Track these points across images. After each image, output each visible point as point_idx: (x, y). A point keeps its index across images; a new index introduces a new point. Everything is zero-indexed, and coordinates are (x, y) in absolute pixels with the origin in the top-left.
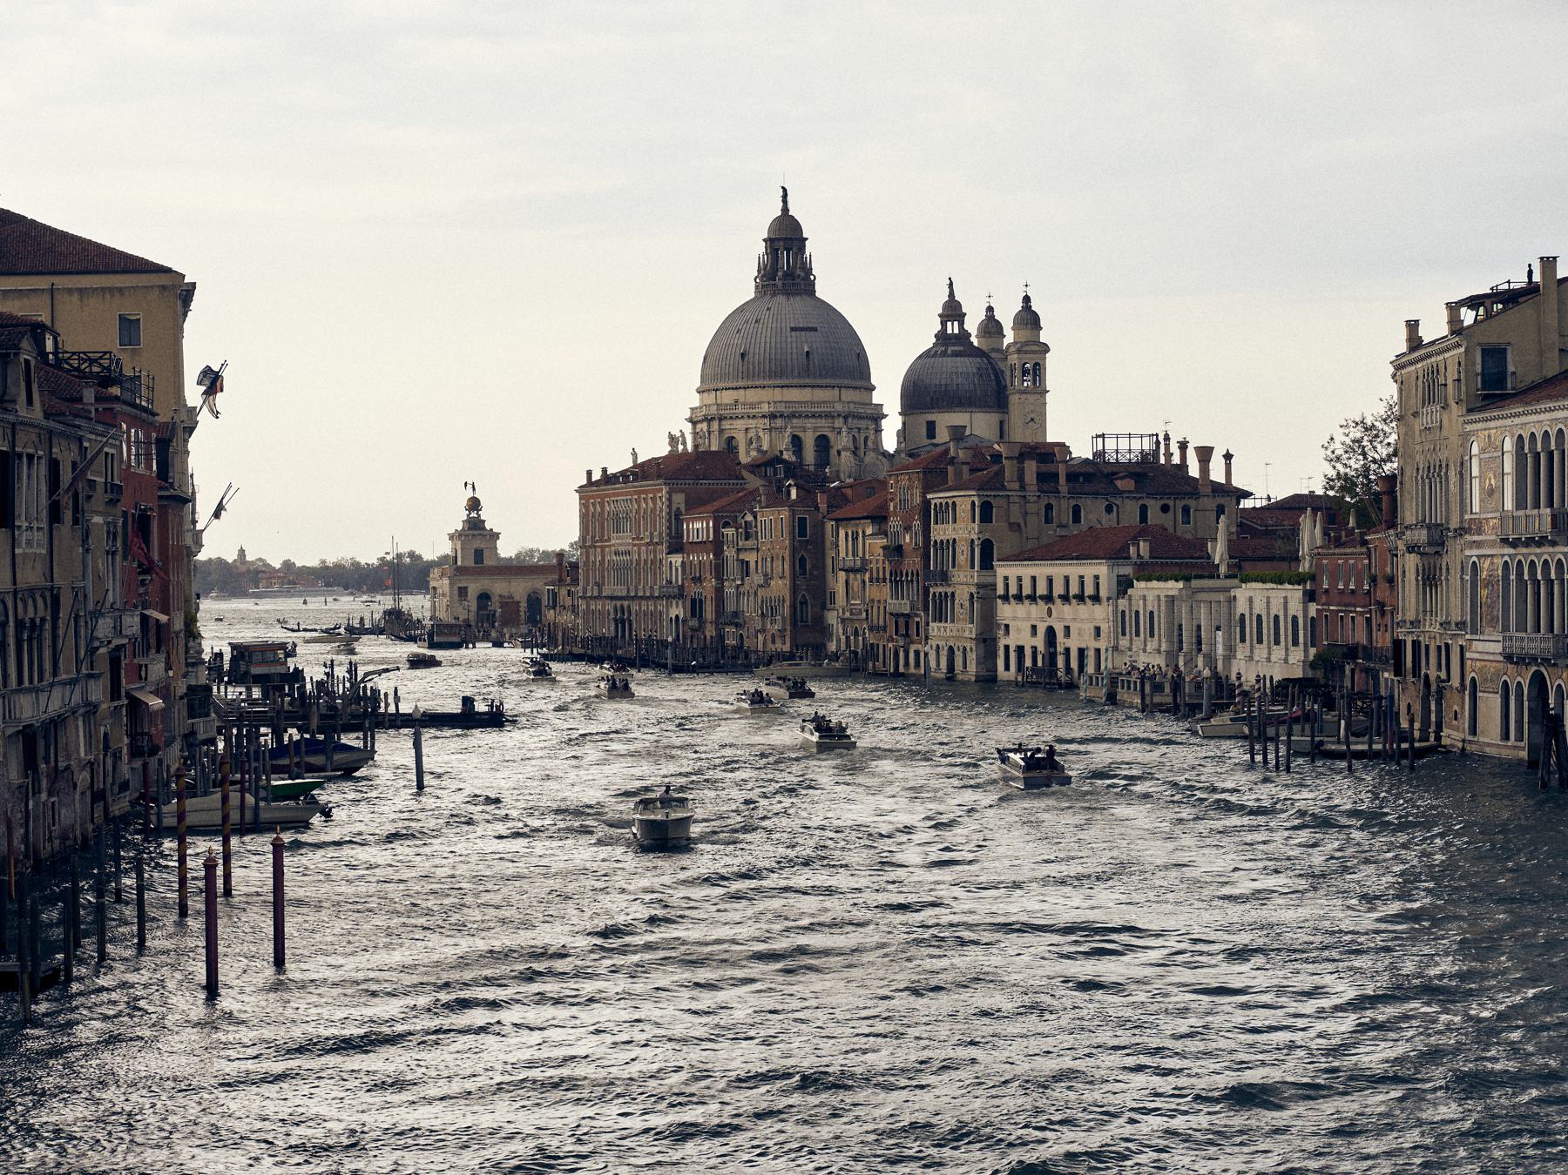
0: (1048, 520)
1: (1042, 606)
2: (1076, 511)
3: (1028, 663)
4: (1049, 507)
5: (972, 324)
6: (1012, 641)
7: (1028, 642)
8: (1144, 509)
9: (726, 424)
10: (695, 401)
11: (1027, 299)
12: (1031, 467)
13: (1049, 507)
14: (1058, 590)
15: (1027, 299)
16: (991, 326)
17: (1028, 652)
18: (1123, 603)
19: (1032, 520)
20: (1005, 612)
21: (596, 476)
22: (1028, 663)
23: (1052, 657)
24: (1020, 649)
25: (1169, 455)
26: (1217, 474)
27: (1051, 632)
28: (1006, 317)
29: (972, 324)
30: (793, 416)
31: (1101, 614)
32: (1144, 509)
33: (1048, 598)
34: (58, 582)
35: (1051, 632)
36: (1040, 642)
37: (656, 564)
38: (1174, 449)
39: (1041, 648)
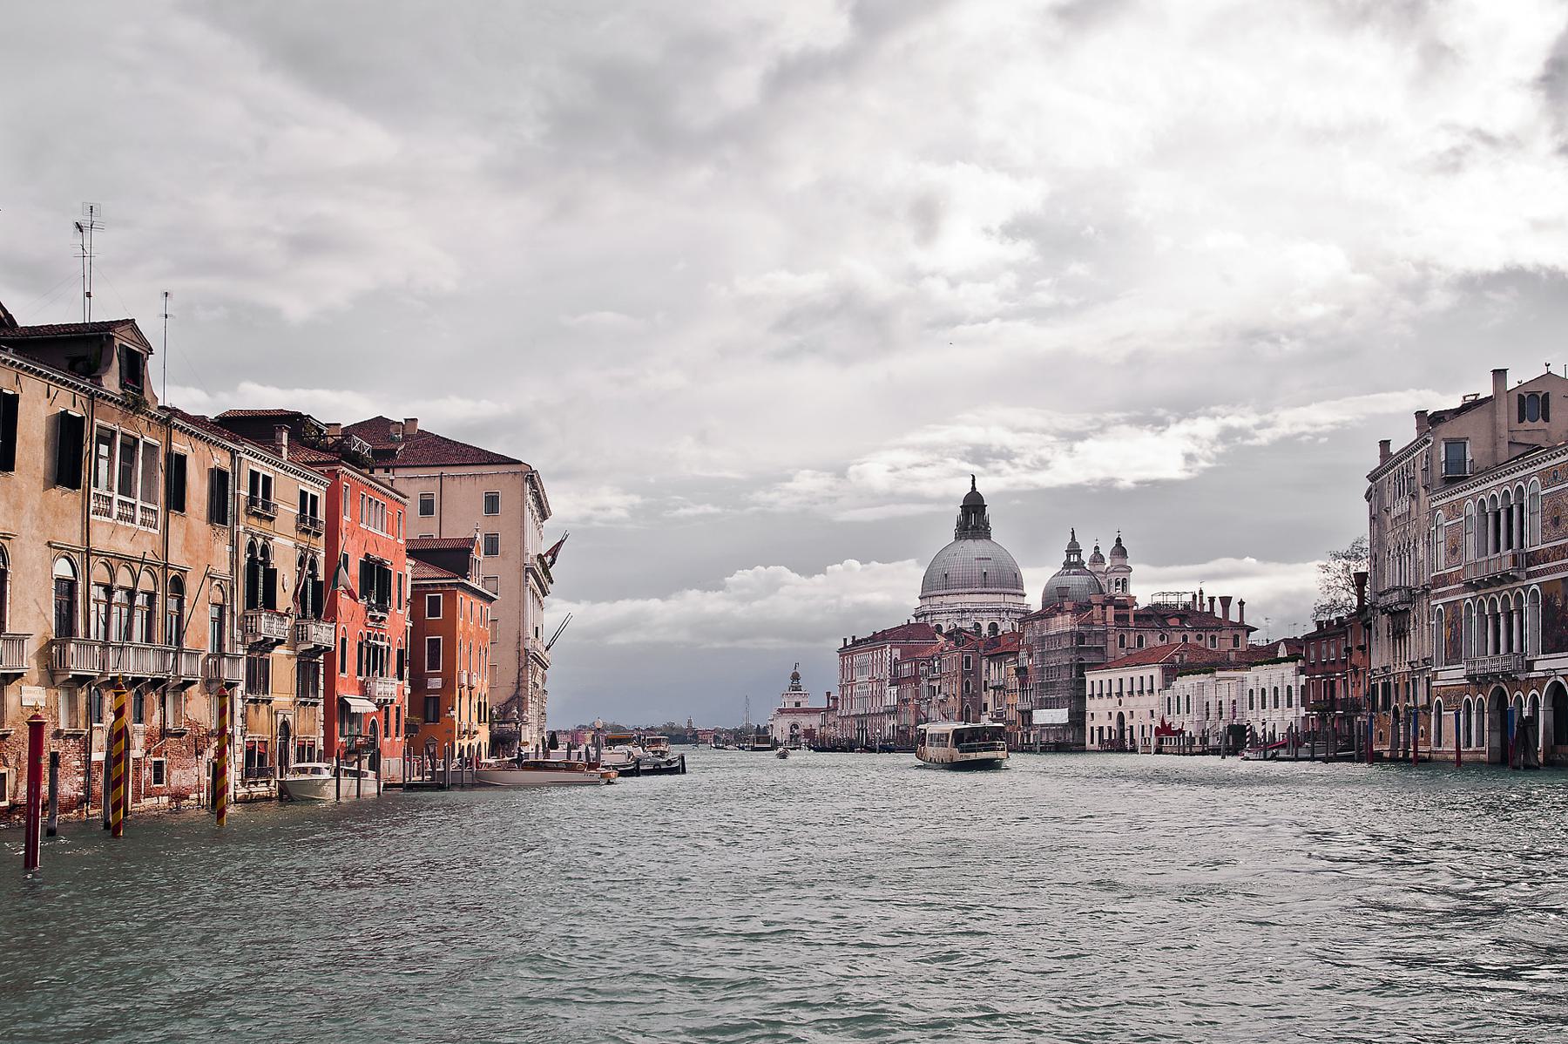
0: (1122, 645)
1: (1115, 699)
2: (1140, 638)
3: (1106, 737)
4: (1122, 637)
5: (1086, 556)
6: (1096, 724)
7: (1106, 724)
8: (1185, 638)
9: (937, 617)
10: (918, 603)
11: (1119, 540)
12: (1111, 610)
13: (1122, 637)
14: (1126, 688)
15: (1119, 540)
16: (1098, 558)
17: (1106, 731)
18: (1168, 693)
19: (1111, 645)
20: (1091, 705)
21: (849, 643)
22: (1106, 737)
23: (1122, 732)
24: (1101, 729)
25: (1202, 605)
26: (1234, 617)
27: (1121, 715)
28: (1106, 552)
29: (1086, 556)
30: (976, 611)
31: (1153, 701)
32: (1185, 638)
33: (1120, 694)
34: (176, 558)
35: (1121, 715)
36: (1114, 724)
37: (882, 694)
38: (1206, 601)
39: (1114, 727)
